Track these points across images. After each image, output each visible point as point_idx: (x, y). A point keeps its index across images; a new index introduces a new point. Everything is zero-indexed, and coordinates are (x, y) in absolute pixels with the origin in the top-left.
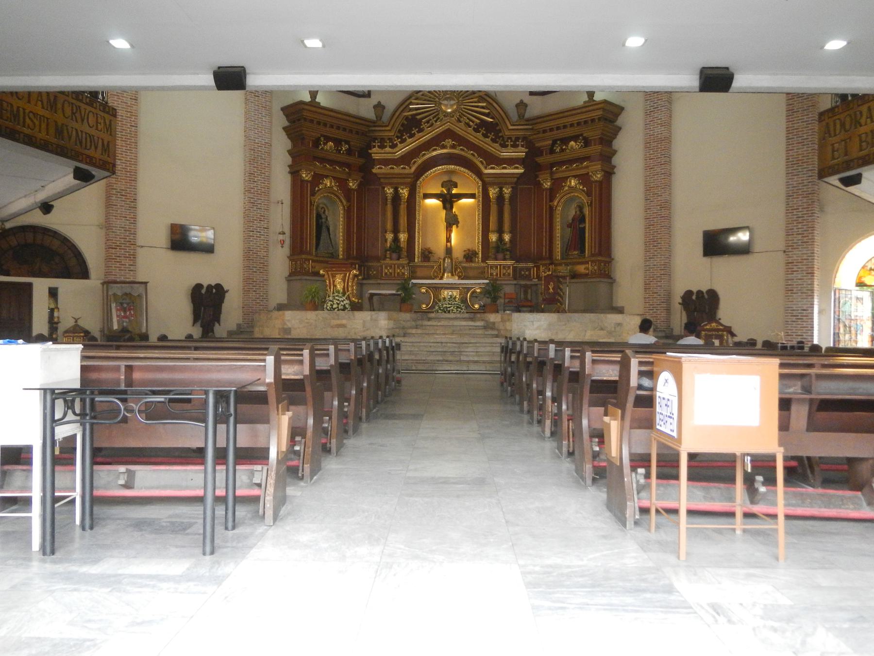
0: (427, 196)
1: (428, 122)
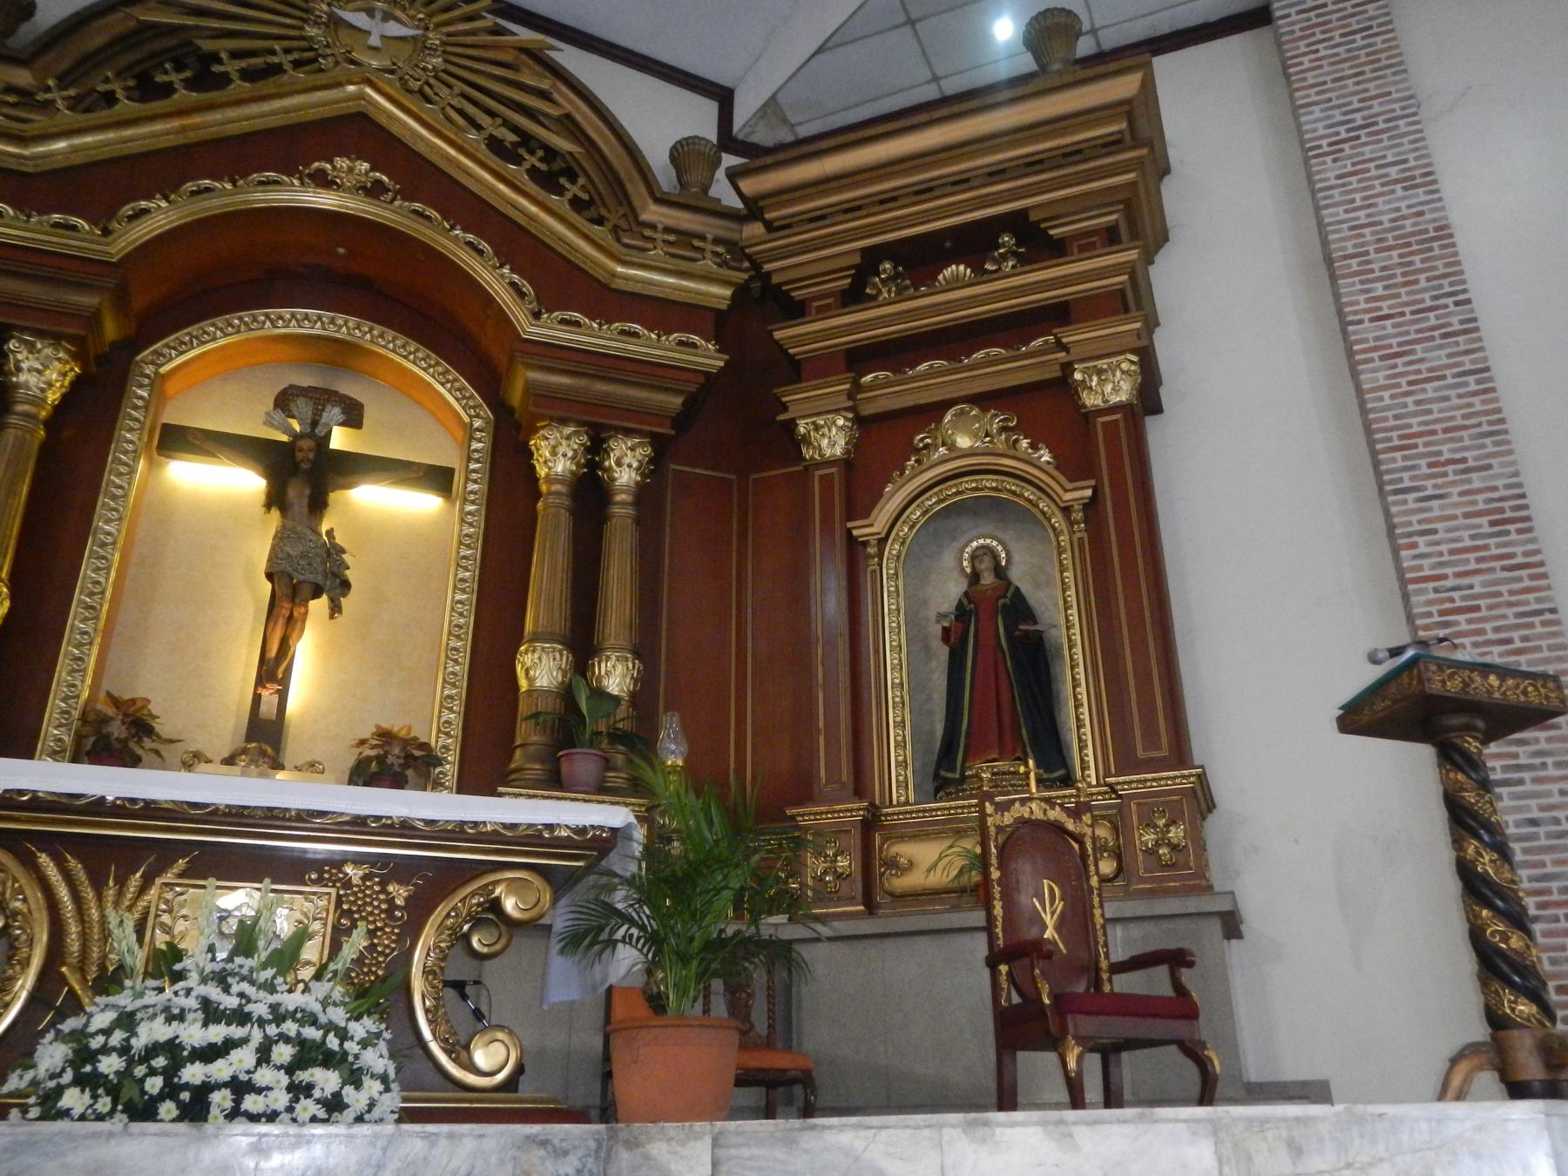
0: (175, 440)
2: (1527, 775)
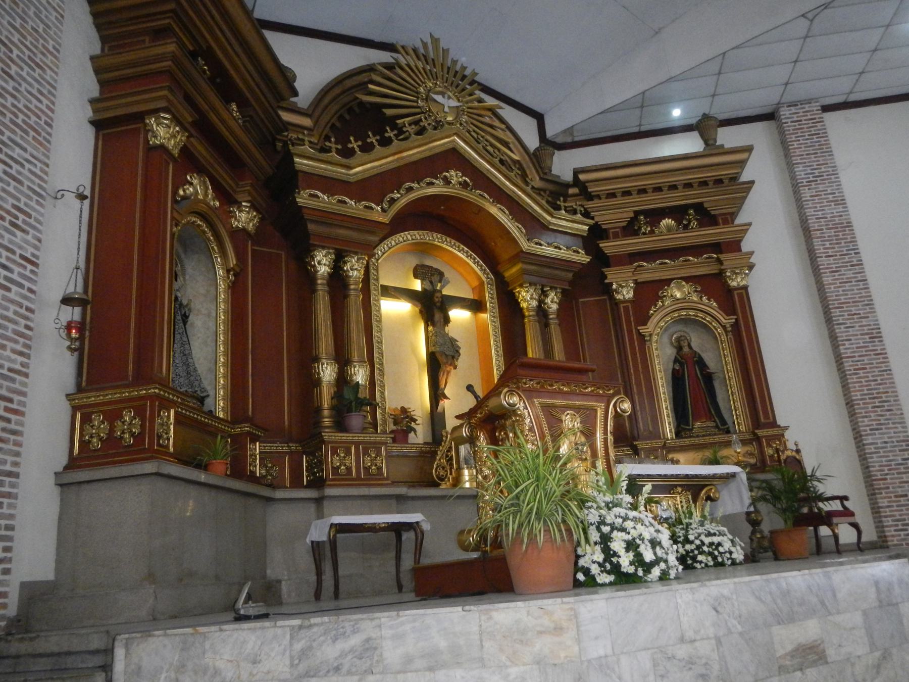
2: (883, 427)
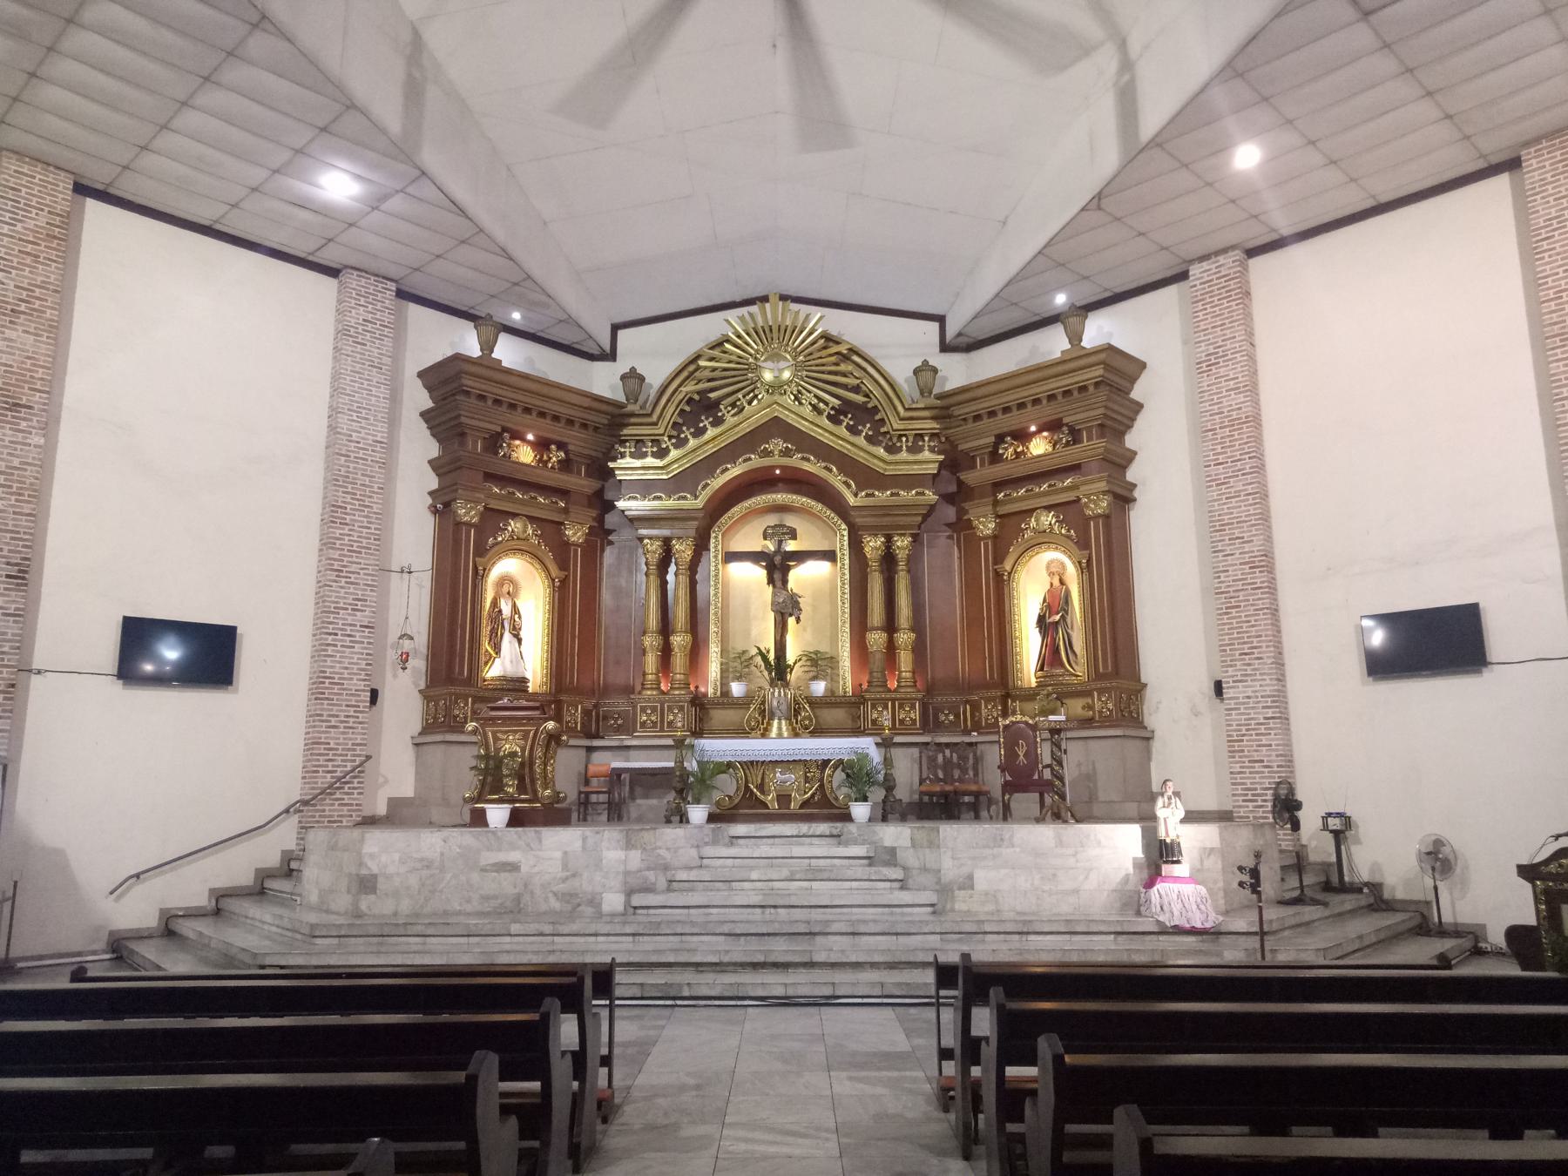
0: (731, 557)
1: (733, 405)
2: (1249, 678)
